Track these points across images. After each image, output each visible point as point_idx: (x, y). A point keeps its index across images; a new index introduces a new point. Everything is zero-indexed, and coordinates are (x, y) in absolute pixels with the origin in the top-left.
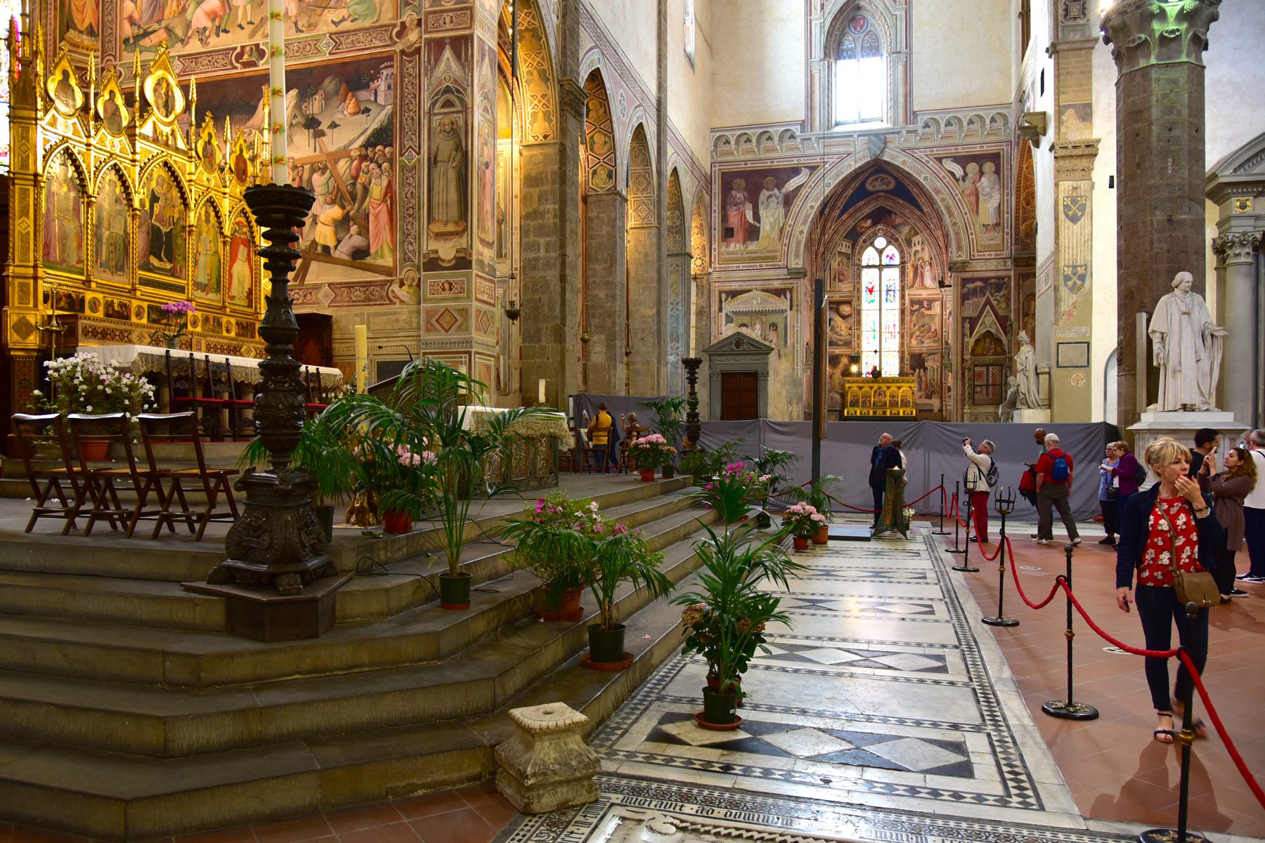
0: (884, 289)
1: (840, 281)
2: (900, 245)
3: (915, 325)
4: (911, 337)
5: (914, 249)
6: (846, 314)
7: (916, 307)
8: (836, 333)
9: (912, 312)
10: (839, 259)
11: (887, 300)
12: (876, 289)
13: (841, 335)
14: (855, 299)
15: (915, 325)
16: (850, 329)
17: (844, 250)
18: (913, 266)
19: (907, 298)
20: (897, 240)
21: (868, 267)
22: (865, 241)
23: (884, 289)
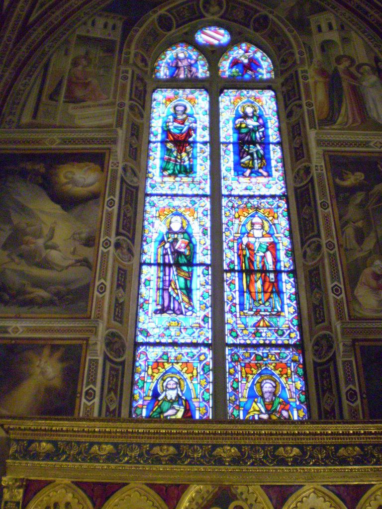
0: (227, 133)
1: (72, 99)
2: (273, 35)
3: (360, 237)
4: (353, 280)
5: (317, 39)
6: (79, 191)
7: (352, 179)
8: (30, 258)
9: (343, 195)
10: (77, 51)
11: (239, 168)
12: (202, 135)
13: (45, 264)
14: (119, 150)
15: (360, 237)
16: (90, 242)
17: (98, 32)
18: (322, 72)
19: (315, 151)
20: (262, 23)
21: (173, 83)
22: (165, 23)
23: (227, 133)
